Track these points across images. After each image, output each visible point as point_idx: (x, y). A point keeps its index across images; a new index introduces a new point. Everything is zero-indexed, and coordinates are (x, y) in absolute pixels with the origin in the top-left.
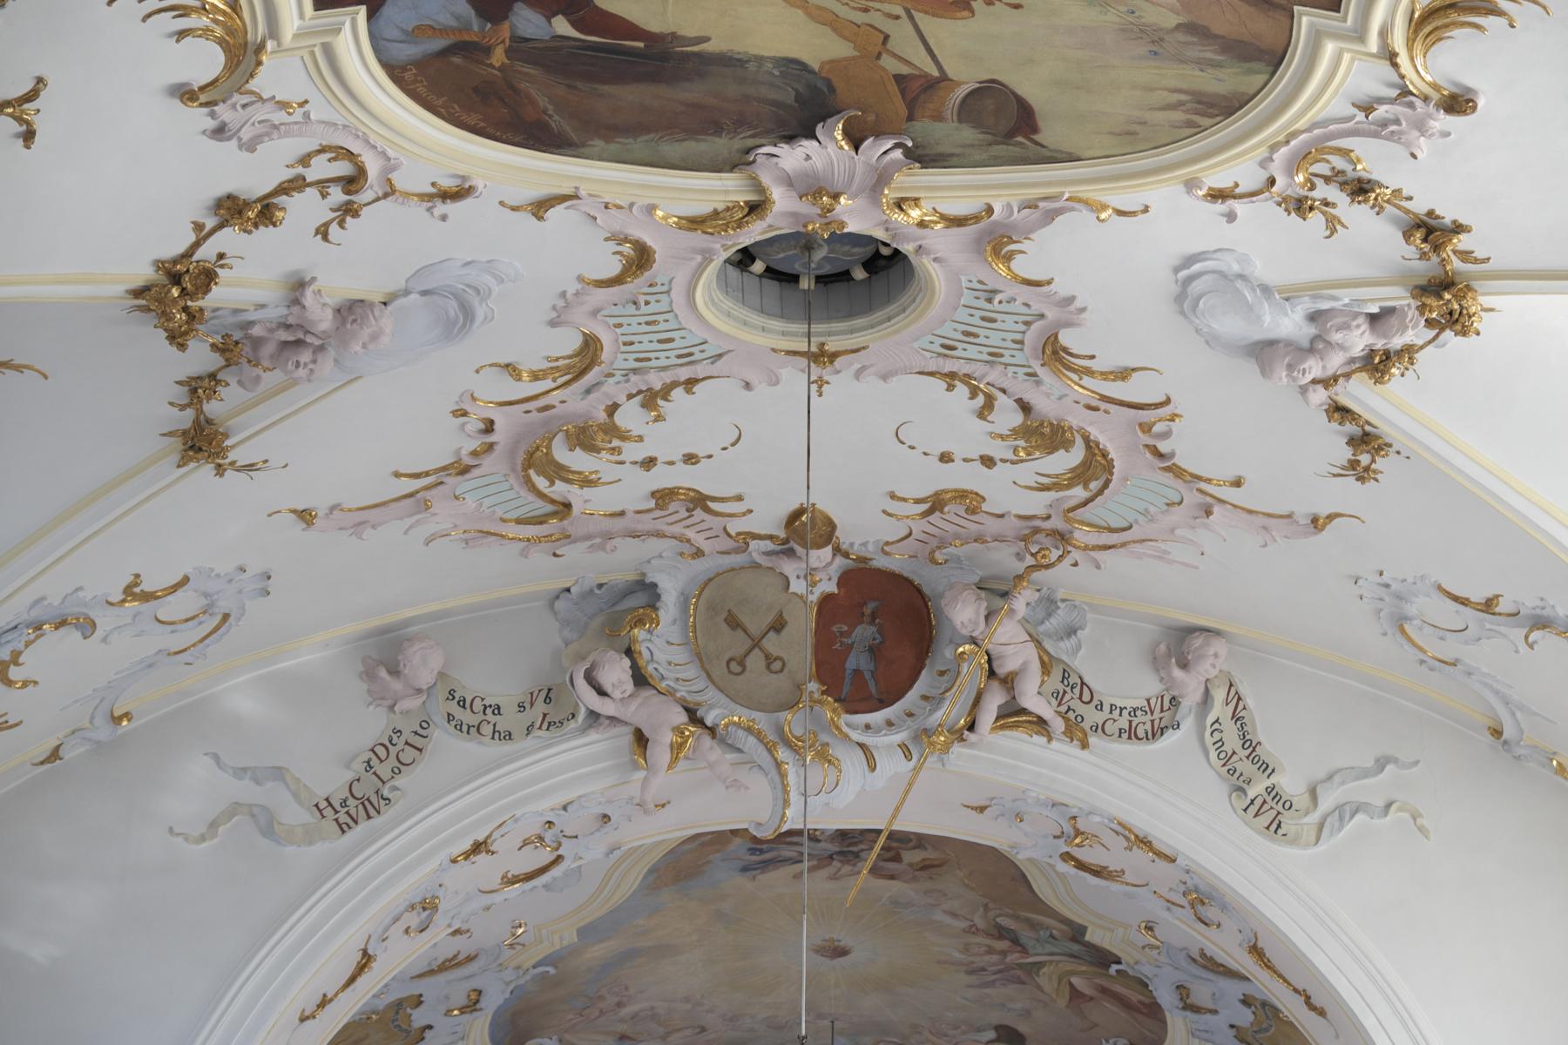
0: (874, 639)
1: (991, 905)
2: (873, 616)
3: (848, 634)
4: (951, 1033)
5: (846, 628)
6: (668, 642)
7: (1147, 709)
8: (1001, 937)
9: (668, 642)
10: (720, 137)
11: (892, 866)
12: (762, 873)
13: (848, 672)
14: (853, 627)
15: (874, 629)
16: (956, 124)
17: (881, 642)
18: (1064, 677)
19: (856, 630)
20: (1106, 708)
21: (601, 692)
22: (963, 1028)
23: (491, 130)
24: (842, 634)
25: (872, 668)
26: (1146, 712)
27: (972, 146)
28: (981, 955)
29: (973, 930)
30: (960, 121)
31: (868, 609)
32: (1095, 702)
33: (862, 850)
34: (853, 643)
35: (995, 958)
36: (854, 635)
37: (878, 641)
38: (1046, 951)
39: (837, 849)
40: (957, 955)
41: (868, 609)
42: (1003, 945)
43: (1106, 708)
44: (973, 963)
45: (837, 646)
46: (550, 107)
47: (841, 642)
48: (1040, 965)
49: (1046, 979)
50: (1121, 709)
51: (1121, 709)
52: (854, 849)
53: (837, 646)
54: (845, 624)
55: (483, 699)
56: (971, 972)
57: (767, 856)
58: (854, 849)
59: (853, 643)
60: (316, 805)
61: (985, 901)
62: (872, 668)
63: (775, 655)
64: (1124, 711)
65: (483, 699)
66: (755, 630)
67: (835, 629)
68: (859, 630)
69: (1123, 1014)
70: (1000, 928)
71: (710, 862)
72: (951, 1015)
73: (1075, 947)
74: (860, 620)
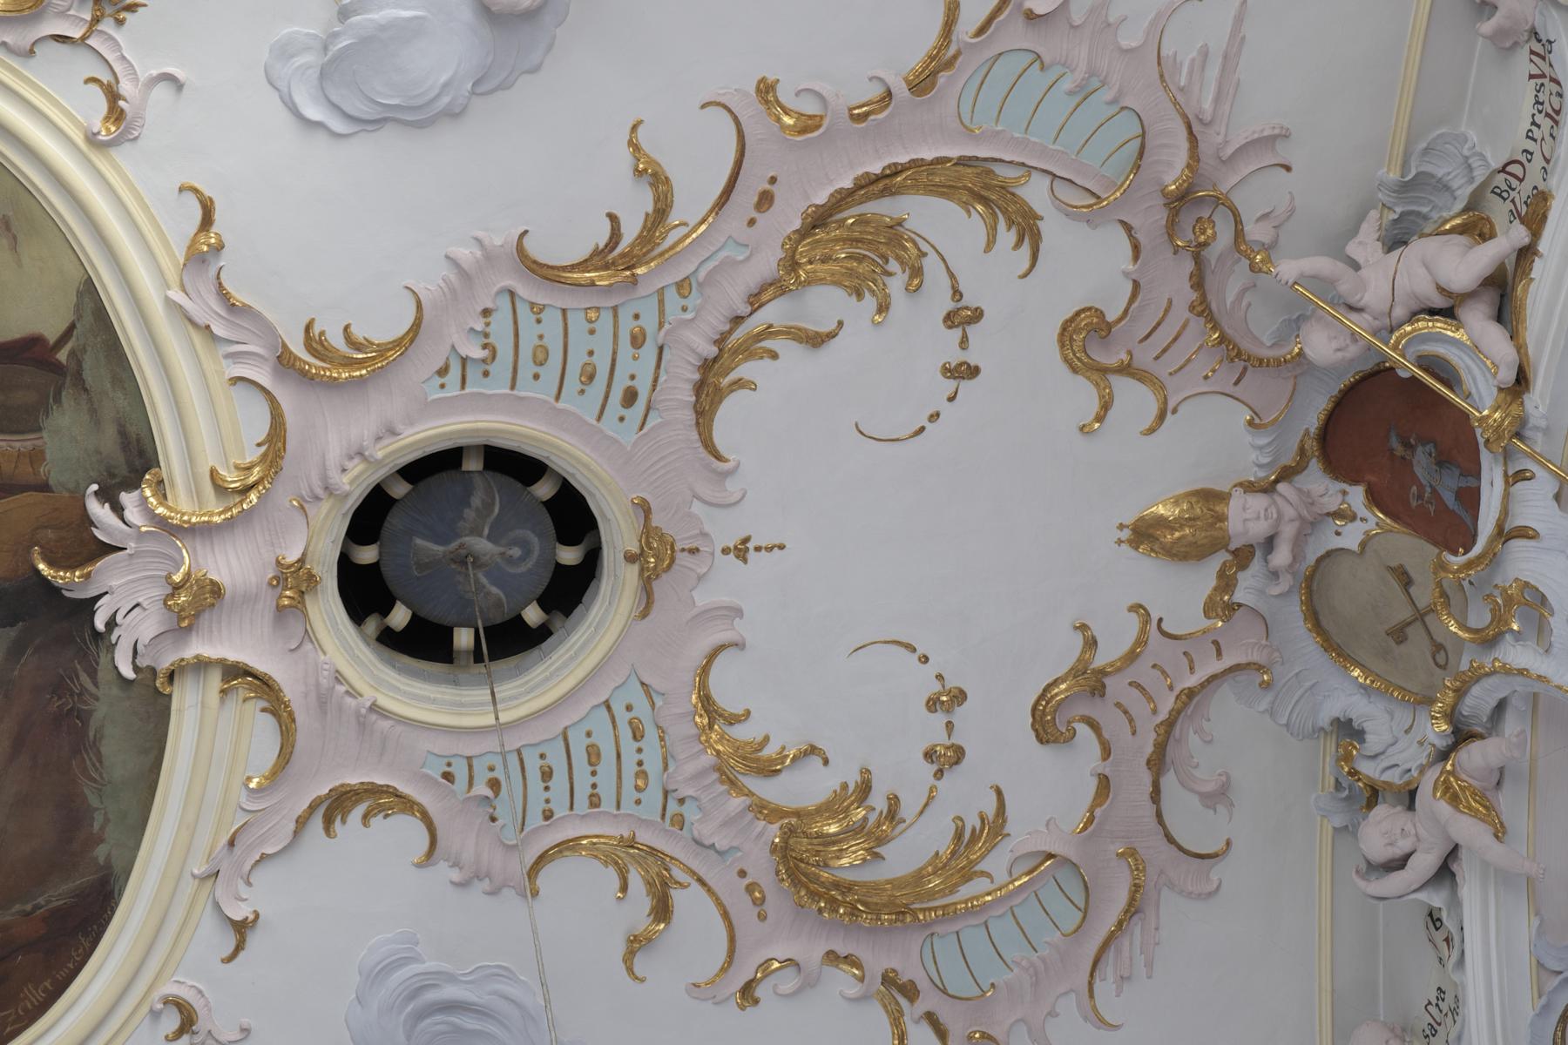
0: (1430, 455)
2: (1407, 445)
3: (1421, 487)
5: (1414, 488)
6: (1407, 732)
7: (1539, 81)
9: (1407, 732)
10: (90, 713)
13: (1456, 508)
14: (1415, 480)
15: (1420, 449)
16: (45, 434)
17: (1435, 447)
18: (1500, 195)
19: (1420, 477)
20: (1530, 145)
21: (1400, 863)
23: (63, 974)
24: (1420, 497)
25: (1457, 473)
26: (1542, 85)
27: (93, 412)
30: (39, 429)
31: (1399, 450)
32: (1523, 159)
34: (1431, 486)
36: (1424, 482)
37: (1433, 450)
41: (1399, 450)
43: (1530, 145)
45: (1432, 509)
46: (17, 907)
47: (1427, 502)
53: (1432, 509)
54: (1410, 488)
55: (1430, 1003)
59: (1431, 486)
66: (1405, 613)
67: (1414, 503)
68: (1419, 471)
74: (1406, 463)
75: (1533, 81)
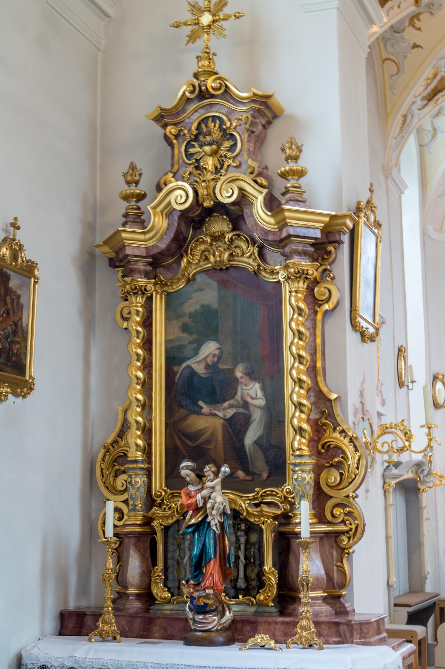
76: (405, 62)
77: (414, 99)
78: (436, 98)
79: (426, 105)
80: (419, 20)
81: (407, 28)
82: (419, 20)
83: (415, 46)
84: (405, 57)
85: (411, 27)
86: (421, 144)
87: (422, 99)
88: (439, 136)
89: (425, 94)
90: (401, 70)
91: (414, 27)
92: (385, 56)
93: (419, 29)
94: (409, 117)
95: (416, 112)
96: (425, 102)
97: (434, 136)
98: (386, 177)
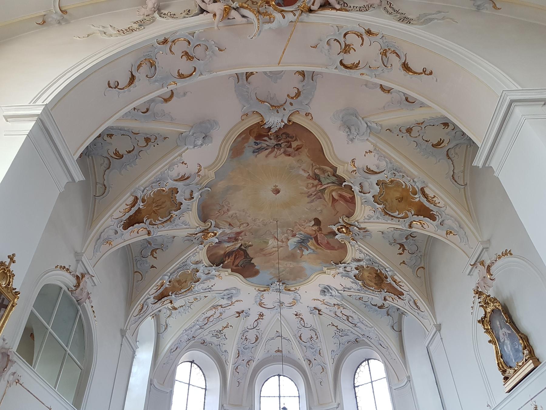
1: (314, 164)
4: (304, 224)
8: (316, 179)
11: (289, 149)
12: (258, 154)
20: (352, 7)
22: (307, 221)
25: (283, 2)
28: (311, 188)
29: (309, 177)
32: (348, 6)
33: (282, 143)
35: (314, 188)
38: (327, 182)
39: (276, 143)
40: (305, 189)
42: (316, 182)
43: (352, 7)
44: (309, 192)
48: (325, 189)
49: (326, 196)
50: (356, 7)
51: (356, 7)
52: (280, 143)
55: (170, 13)
56: (308, 197)
57: (259, 146)
58: (280, 143)
60: (118, 31)
61: (312, 162)
62: (283, 2)
63: (255, 1)
64: (357, 7)
65: (170, 13)
69: (345, 205)
70: (316, 175)
71: (245, 147)
72: (304, 216)
73: (334, 178)
75: (363, 6)
76: (146, 274)
77: (149, 296)
78: (163, 300)
79: (157, 302)
80: (156, 253)
81: (149, 256)
82: (156, 253)
83: (153, 267)
84: (147, 272)
85: (151, 256)
86: (159, 332)
87: (154, 298)
88: (169, 328)
89: (156, 294)
90: (143, 279)
91: (153, 256)
92: (135, 270)
93: (156, 258)
94: (145, 307)
95: (150, 305)
96: (156, 301)
97: (166, 329)
98: (123, 336)
